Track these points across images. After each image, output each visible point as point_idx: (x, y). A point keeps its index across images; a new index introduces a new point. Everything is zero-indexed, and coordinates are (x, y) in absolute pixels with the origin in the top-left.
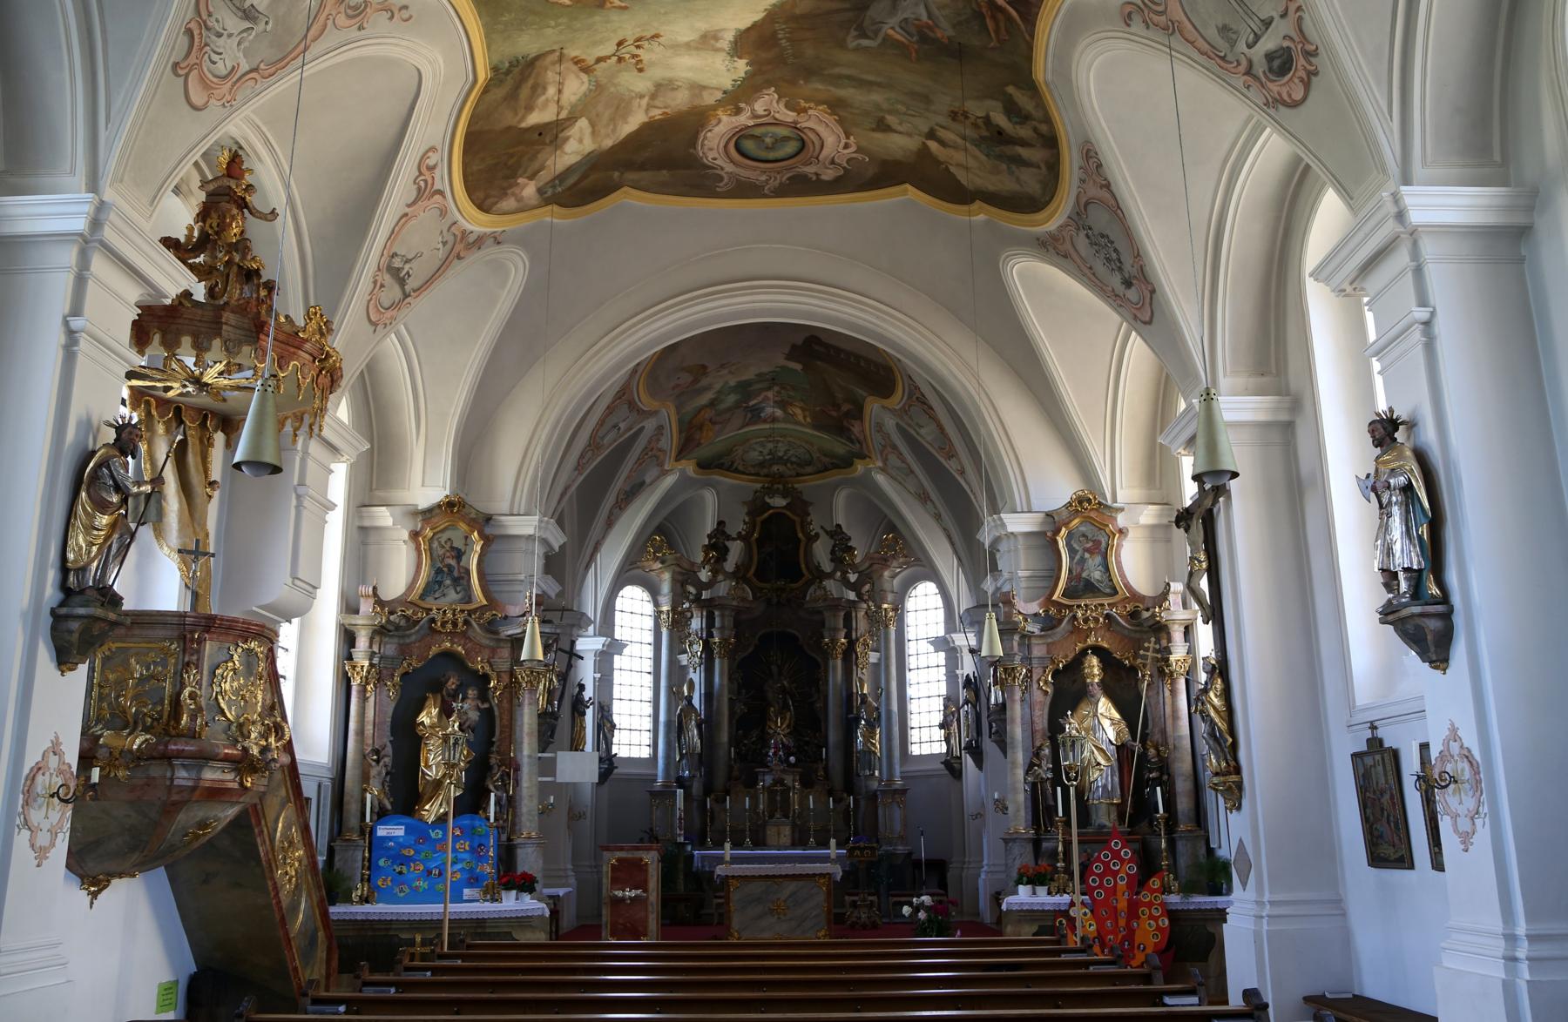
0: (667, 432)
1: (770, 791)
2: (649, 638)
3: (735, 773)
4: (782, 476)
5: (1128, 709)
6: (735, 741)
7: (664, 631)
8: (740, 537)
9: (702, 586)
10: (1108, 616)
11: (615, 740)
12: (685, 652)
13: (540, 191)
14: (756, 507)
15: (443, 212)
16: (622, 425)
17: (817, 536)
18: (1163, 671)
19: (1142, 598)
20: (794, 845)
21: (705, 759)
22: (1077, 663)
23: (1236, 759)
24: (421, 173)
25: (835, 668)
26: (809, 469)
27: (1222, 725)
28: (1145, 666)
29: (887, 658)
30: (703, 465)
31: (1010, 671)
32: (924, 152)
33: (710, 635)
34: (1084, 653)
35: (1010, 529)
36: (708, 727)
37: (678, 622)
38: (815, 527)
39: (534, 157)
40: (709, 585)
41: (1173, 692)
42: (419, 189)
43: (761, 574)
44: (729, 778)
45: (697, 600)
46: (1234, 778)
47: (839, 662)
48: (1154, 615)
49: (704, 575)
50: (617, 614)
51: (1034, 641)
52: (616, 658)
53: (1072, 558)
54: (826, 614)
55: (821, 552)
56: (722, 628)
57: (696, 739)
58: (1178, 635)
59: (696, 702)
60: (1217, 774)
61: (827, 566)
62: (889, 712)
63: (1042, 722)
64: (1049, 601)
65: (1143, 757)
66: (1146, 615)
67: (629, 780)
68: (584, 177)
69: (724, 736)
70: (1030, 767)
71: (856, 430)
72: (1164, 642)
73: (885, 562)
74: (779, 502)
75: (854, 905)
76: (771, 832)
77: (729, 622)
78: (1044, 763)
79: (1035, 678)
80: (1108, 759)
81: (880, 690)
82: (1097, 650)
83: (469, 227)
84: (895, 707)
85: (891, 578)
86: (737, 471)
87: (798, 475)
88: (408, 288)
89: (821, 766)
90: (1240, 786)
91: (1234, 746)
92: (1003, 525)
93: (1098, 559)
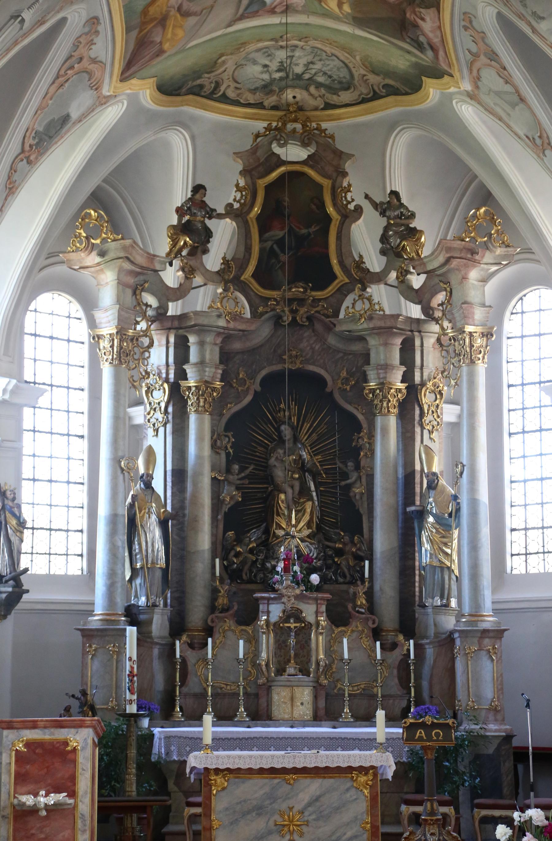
0: (104, 27)
1: (279, 630)
2: (82, 378)
3: (222, 601)
4: (301, 109)
6: (222, 549)
7: (107, 371)
8: (230, 212)
9: (167, 294)
11: (25, 547)
12: (139, 403)
14: (257, 163)
16: (27, 15)
17: (359, 210)
20: (317, 718)
21: (173, 577)
25: (385, 431)
26: (345, 97)
29: (472, 415)
30: (169, 89)
33: (182, 375)
36: (175, 526)
37: (129, 351)
38: (355, 197)
40: (180, 293)
43: (264, 276)
44: (212, 608)
45: (161, 316)
47: (392, 421)
49: (171, 276)
50: (28, 341)
52: (27, 412)
54: (373, 342)
55: (365, 238)
56: (201, 363)
57: (159, 545)
59: (158, 484)
61: (375, 262)
62: (474, 503)
67: (47, 612)
69: (204, 540)
71: (427, 27)
73: (471, 254)
74: (295, 153)
75: (416, 819)
76: (279, 697)
77: (212, 354)
81: (459, 469)
84: (483, 495)
85: (480, 282)
86: (225, 99)
87: (328, 106)
89: (361, 590)
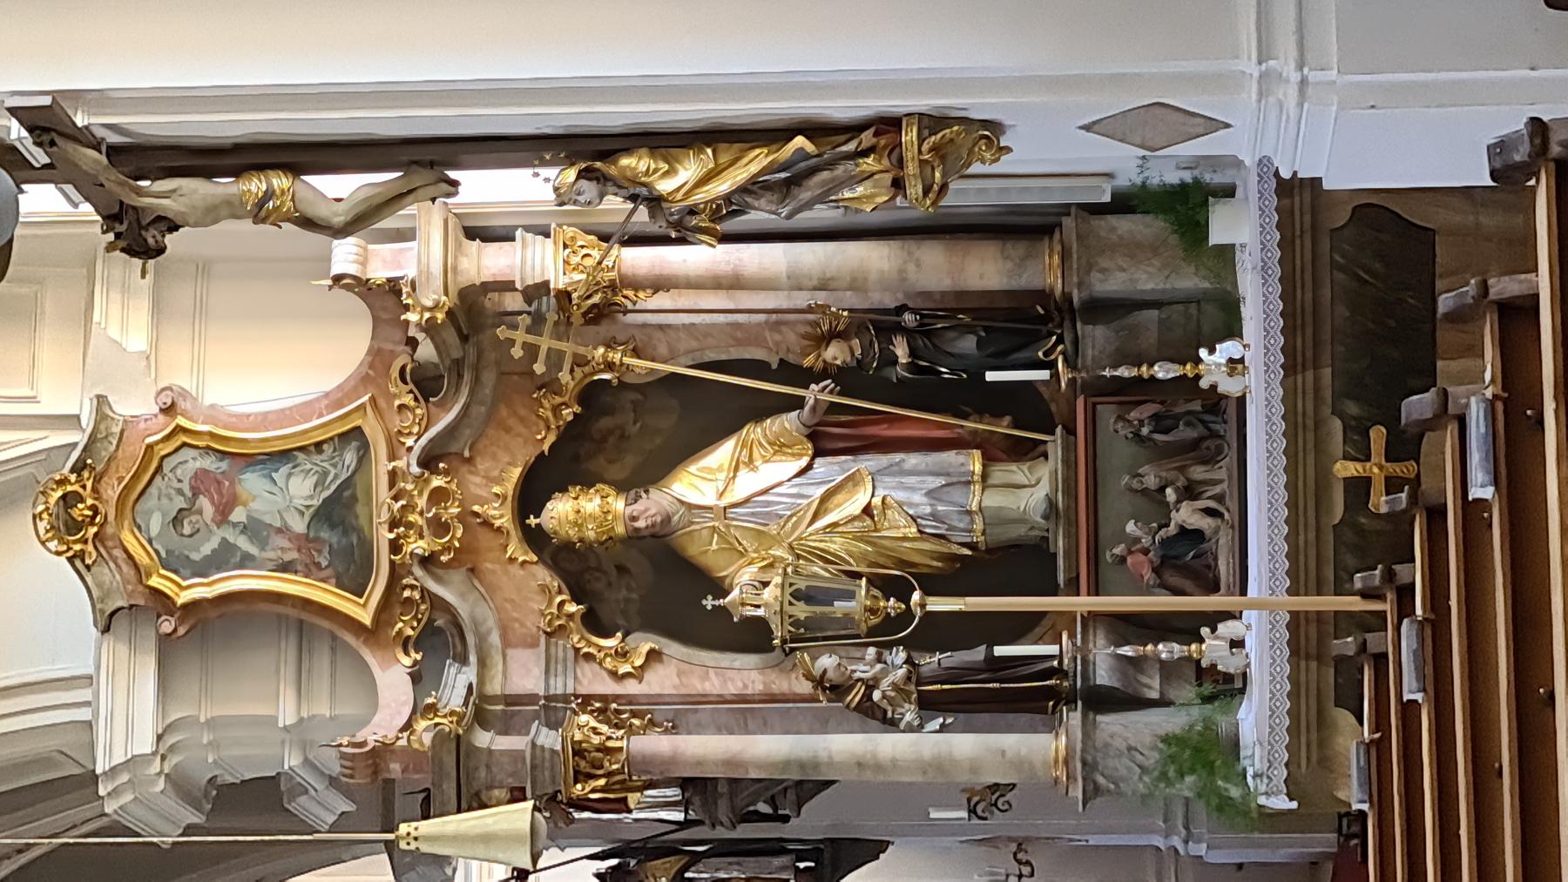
5: (707, 407)
10: (428, 462)
18: (602, 308)
19: (377, 358)
22: (571, 562)
23: (853, 129)
27: (756, 162)
28: (580, 361)
31: (584, 760)
34: (536, 539)
35: (145, 745)
41: (659, 284)
46: (909, 136)
48: (430, 328)
51: (495, 687)
53: (246, 561)
58: (491, 262)
60: (898, 185)
63: (740, 673)
64: (372, 634)
65: (845, 378)
66: (426, 351)
70: (877, 716)
72: (513, 302)
78: (863, 671)
79: (609, 687)
80: (852, 481)
82: (530, 497)
90: (932, 122)
91: (817, 130)
92: (133, 762)
93: (252, 482)
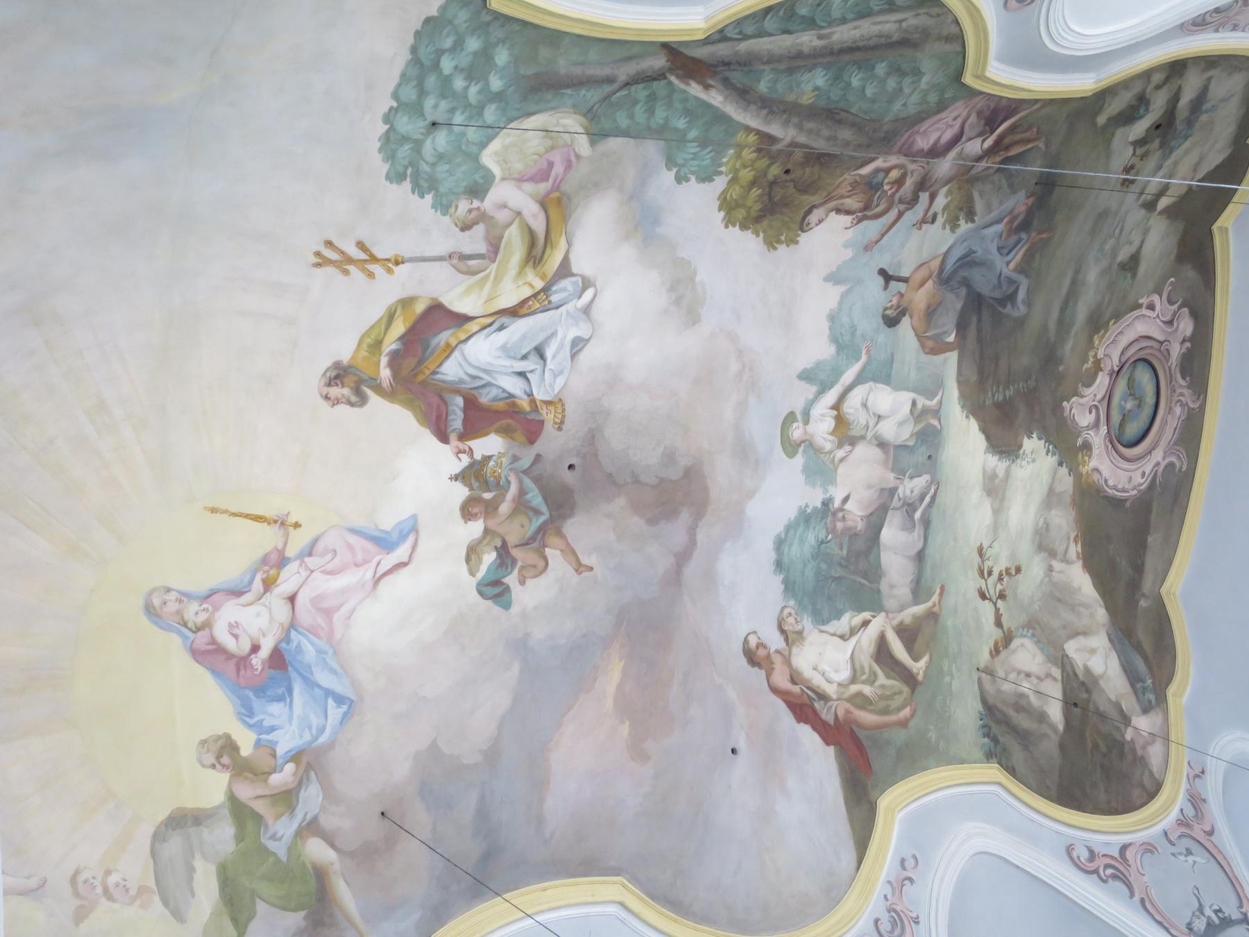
13: (1146, 711)
15: (1149, 848)
24: (1096, 872)
32: (1170, 212)
39: (1102, 716)
42: (1114, 877)
68: (1138, 648)
83: (1174, 814)
88: (1236, 915)
